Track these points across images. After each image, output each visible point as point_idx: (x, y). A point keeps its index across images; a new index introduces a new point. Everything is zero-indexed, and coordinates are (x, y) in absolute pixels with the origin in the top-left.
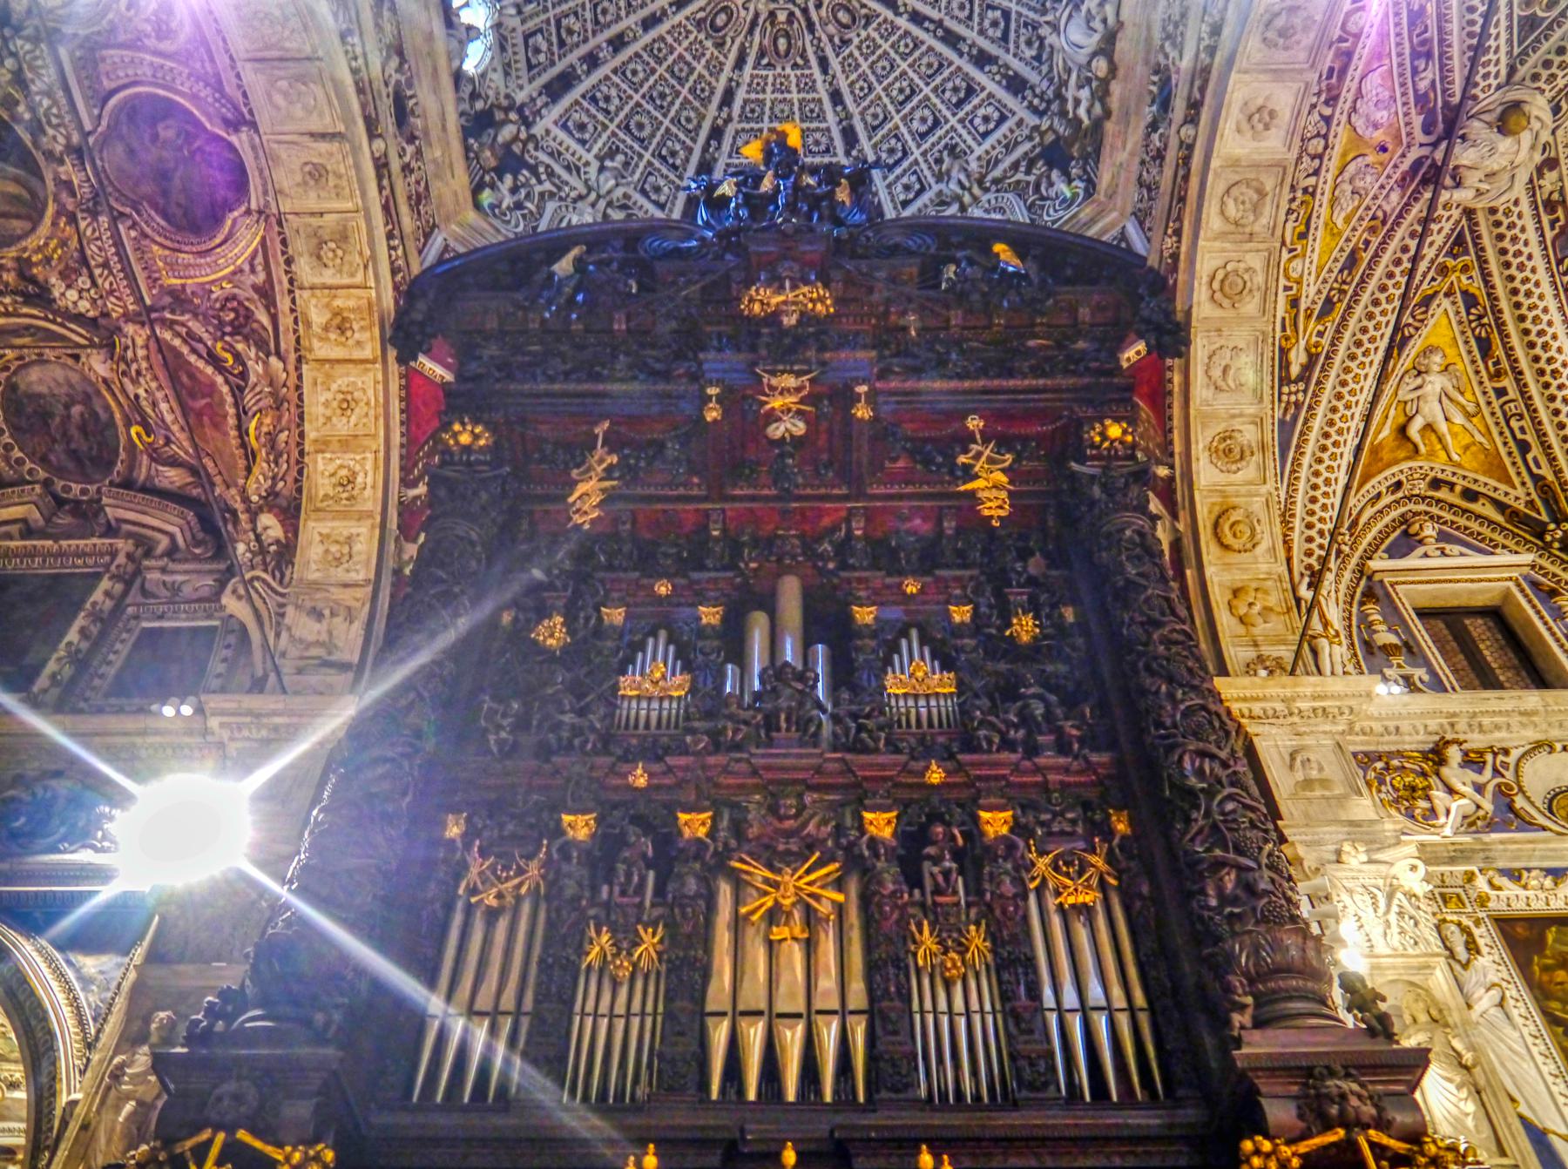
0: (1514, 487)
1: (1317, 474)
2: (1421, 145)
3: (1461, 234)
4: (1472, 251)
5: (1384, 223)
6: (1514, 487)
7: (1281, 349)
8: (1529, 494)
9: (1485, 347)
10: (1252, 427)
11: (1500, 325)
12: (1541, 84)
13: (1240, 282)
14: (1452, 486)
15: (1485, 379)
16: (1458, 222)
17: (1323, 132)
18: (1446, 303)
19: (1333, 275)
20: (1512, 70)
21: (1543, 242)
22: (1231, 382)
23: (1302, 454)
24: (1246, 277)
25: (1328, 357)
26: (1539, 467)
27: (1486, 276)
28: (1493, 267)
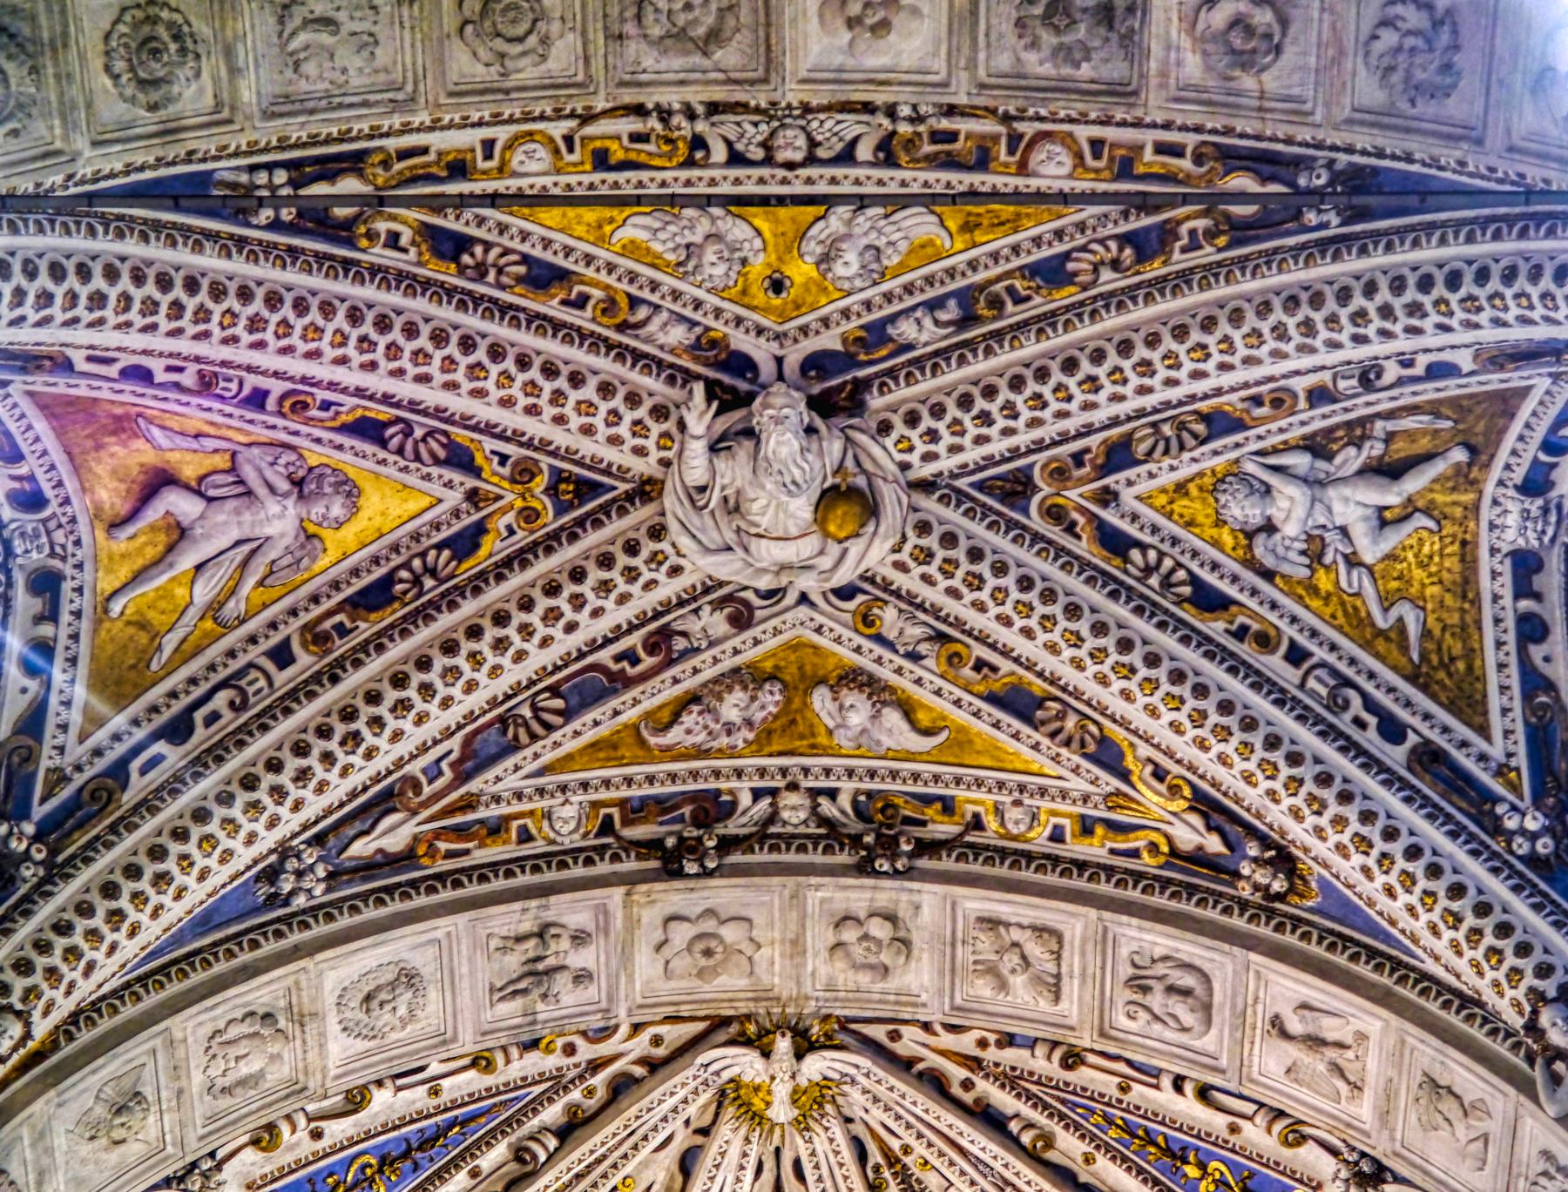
0: (82, 739)
1: (111, 274)
2: (779, 361)
3: (595, 488)
4: (566, 519)
5: (622, 327)
6: (82, 739)
7: (360, 156)
8: (79, 768)
9: (376, 596)
10: (209, 101)
11: (424, 615)
12: (913, 540)
13: (520, 30)
14: (52, 616)
15: (305, 618)
16: (622, 473)
17: (822, 153)
18: (454, 498)
19: (516, 244)
20: (926, 486)
21: (594, 646)
22: (303, 38)
23: (145, 238)
24: (532, 40)
25: (347, 263)
26: (143, 771)
27: (521, 558)
28: (543, 566)
